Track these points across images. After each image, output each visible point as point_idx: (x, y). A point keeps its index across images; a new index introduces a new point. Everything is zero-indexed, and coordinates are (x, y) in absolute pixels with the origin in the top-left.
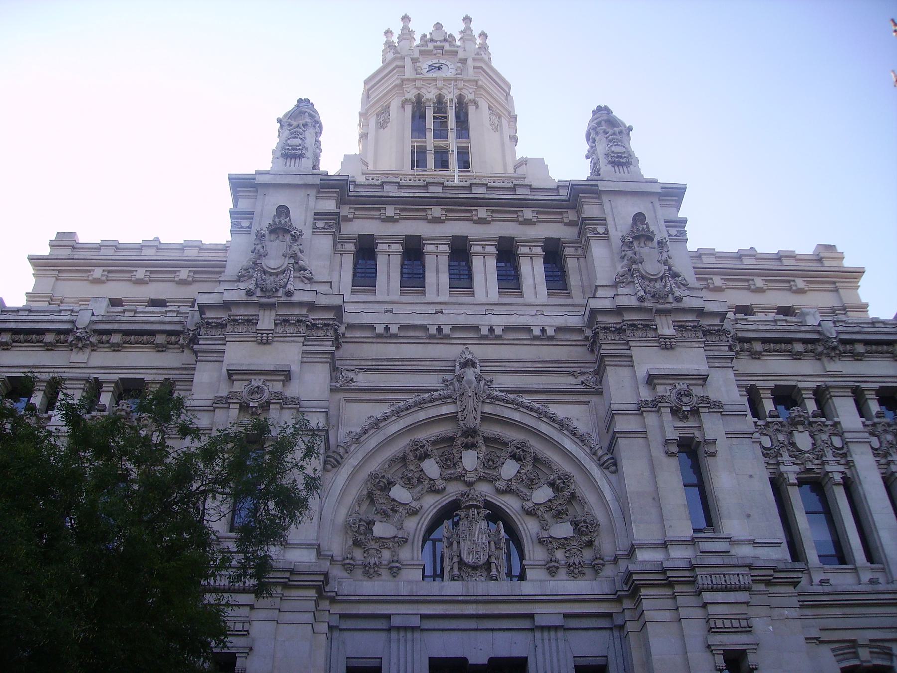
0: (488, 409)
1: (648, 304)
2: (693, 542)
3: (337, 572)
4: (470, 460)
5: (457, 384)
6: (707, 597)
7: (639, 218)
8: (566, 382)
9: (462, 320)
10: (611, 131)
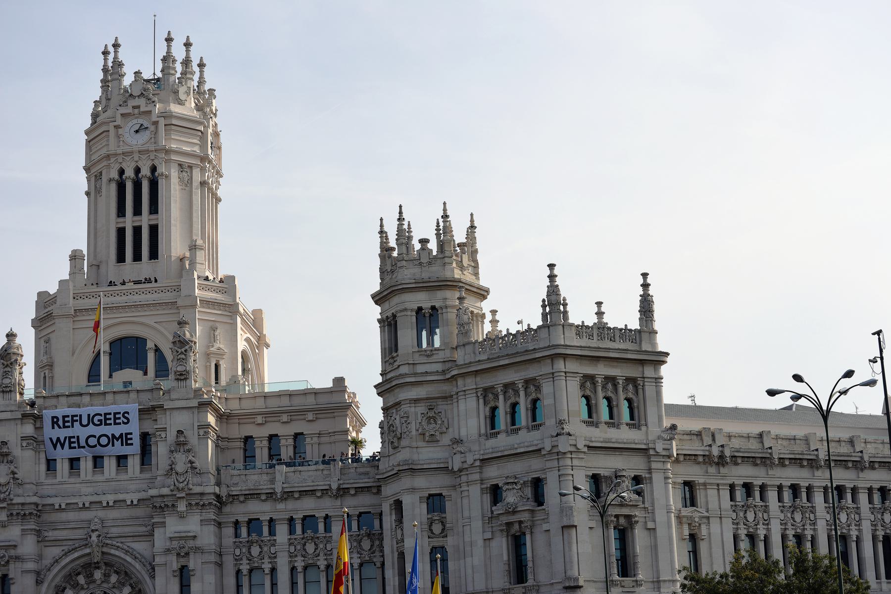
0: (105, 550)
1: (174, 493)
4: (98, 575)
5: (89, 538)
7: (179, 432)
8: (144, 529)
10: (180, 351)
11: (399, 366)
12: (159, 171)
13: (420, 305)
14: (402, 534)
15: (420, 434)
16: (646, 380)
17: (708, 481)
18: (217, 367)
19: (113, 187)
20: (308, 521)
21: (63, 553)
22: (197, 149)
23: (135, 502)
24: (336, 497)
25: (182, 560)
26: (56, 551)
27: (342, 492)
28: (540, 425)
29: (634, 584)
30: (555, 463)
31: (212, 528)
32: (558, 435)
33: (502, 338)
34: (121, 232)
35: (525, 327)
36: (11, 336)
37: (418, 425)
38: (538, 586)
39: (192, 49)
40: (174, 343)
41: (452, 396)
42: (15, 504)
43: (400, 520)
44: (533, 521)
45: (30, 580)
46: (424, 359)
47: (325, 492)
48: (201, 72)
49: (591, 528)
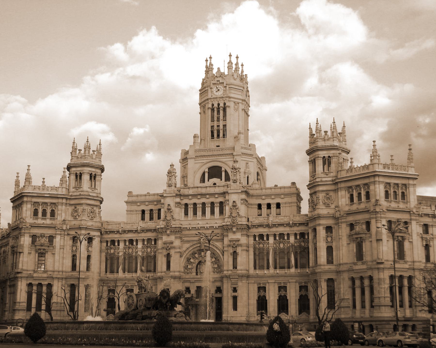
1: (231, 224)
2: (231, 270)
3: (183, 274)
6: (232, 280)
7: (233, 201)
9: (202, 226)
11: (316, 178)
12: (227, 104)
13: (324, 156)
14: (316, 241)
15: (324, 204)
16: (410, 185)
17: (433, 224)
18: (248, 177)
19: (210, 111)
20: (282, 235)
21: (190, 245)
22: (240, 97)
23: (217, 227)
24: (291, 227)
25: (234, 249)
26: (187, 245)
27: (295, 225)
28: (369, 201)
29: (404, 262)
30: (375, 216)
31: (245, 237)
32: (376, 205)
33: (355, 168)
34: (212, 127)
35: (364, 165)
36: (172, 166)
37: (323, 200)
38: (367, 262)
39: (239, 59)
40: (232, 169)
41: (335, 190)
42: (172, 227)
43: (315, 236)
44: (366, 237)
45: (178, 255)
46: (326, 176)
47: (288, 225)
48: (242, 68)
49: (388, 241)
